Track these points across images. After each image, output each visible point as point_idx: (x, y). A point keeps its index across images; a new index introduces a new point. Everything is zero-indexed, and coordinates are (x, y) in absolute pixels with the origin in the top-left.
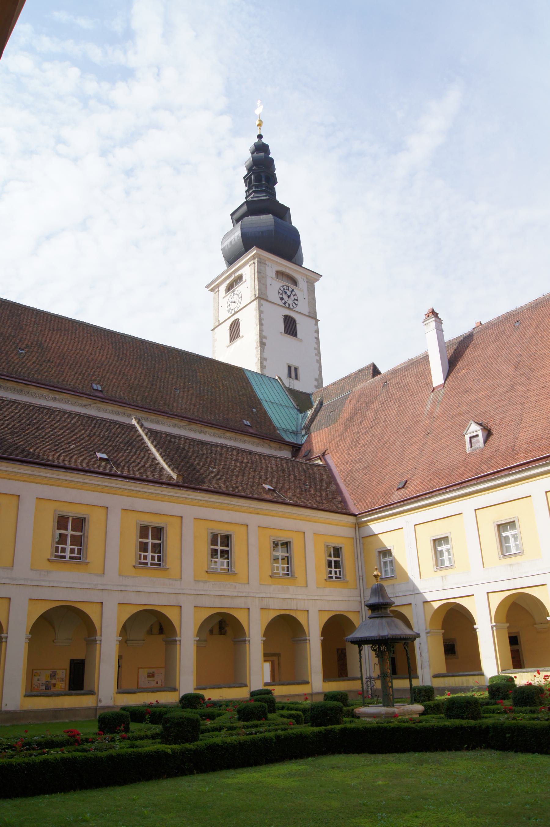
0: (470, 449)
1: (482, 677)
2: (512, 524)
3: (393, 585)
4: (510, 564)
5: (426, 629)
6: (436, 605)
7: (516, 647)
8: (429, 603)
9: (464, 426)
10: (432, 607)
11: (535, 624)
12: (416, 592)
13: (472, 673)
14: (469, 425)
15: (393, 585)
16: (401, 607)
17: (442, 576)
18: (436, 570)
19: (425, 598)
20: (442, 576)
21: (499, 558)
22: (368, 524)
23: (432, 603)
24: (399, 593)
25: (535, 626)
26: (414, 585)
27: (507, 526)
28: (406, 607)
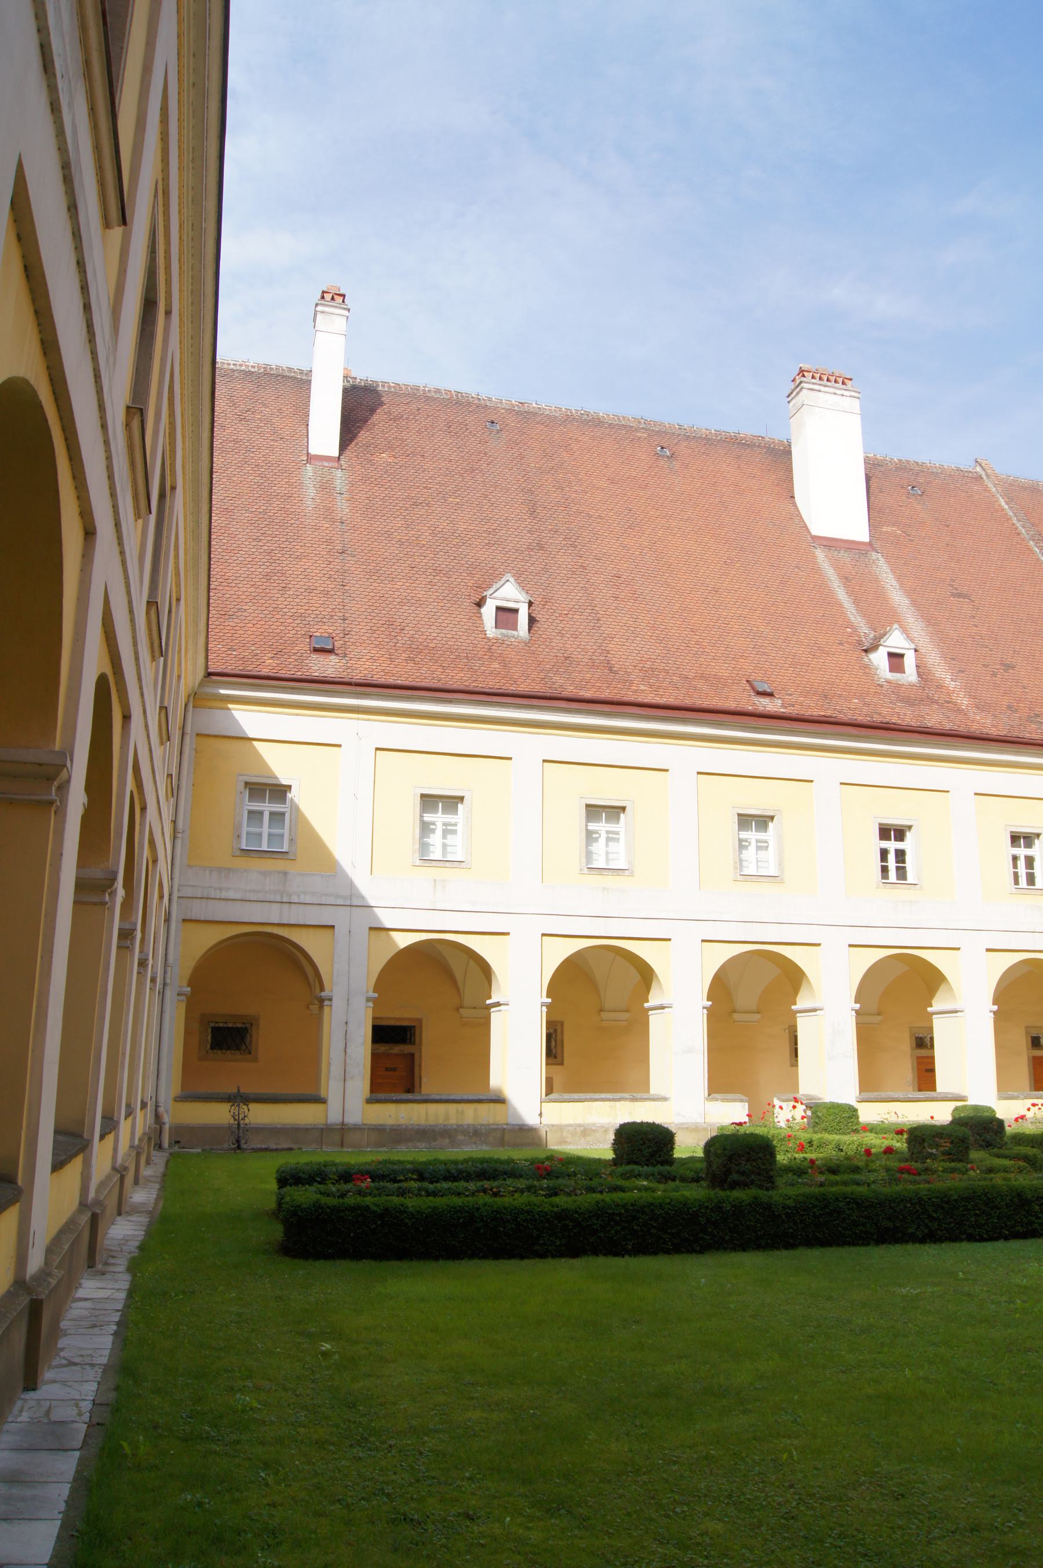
0: (494, 630)
1: (499, 1106)
2: (615, 811)
3: (285, 874)
4: (604, 888)
5: (367, 992)
6: (403, 941)
7: (923, 1052)
8: (383, 934)
9: (491, 578)
10: (393, 943)
11: (734, 1011)
12: (355, 903)
13: (603, 1096)
14: (501, 583)
15: (285, 874)
16: (304, 931)
17: (435, 880)
18: (418, 863)
19: (375, 917)
20: (435, 880)
21: (581, 870)
22: (230, 706)
23: (393, 934)
24: (302, 896)
25: (736, 1016)
26: (351, 885)
27: (752, 821)
28: (311, 931)
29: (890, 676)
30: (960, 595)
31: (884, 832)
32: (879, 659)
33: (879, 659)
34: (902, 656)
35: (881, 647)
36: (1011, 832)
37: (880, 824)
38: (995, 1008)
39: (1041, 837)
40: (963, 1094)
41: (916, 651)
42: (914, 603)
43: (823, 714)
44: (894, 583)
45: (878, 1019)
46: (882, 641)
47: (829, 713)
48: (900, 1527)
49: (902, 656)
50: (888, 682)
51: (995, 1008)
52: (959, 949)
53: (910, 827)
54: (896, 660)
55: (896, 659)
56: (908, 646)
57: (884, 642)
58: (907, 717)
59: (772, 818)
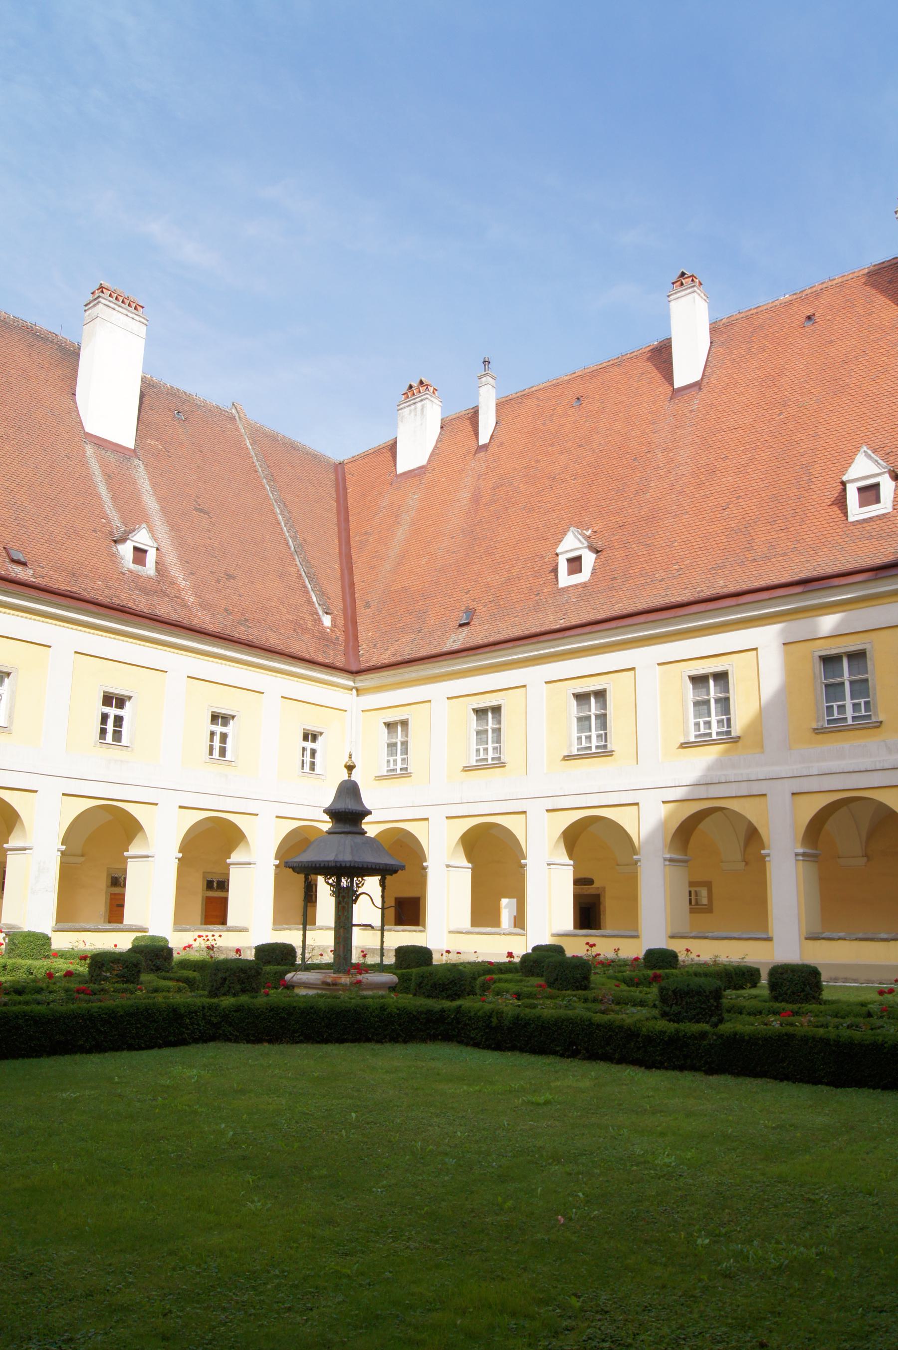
7: (116, 890)
29: (132, 566)
30: (201, 511)
31: (108, 700)
32: (126, 550)
33: (126, 550)
34: (145, 551)
35: (128, 541)
36: (212, 712)
37: (105, 692)
38: (180, 855)
39: (235, 719)
40: (145, 926)
41: (158, 549)
42: (163, 509)
43: (69, 589)
44: (149, 488)
45: (82, 859)
46: (130, 536)
47: (74, 589)
48: (24, 1302)
49: (145, 551)
50: (130, 571)
51: (180, 855)
52: (157, 804)
53: (130, 698)
54: (140, 554)
55: (140, 553)
56: (152, 545)
57: (132, 537)
58: (141, 604)
59: (8, 674)
